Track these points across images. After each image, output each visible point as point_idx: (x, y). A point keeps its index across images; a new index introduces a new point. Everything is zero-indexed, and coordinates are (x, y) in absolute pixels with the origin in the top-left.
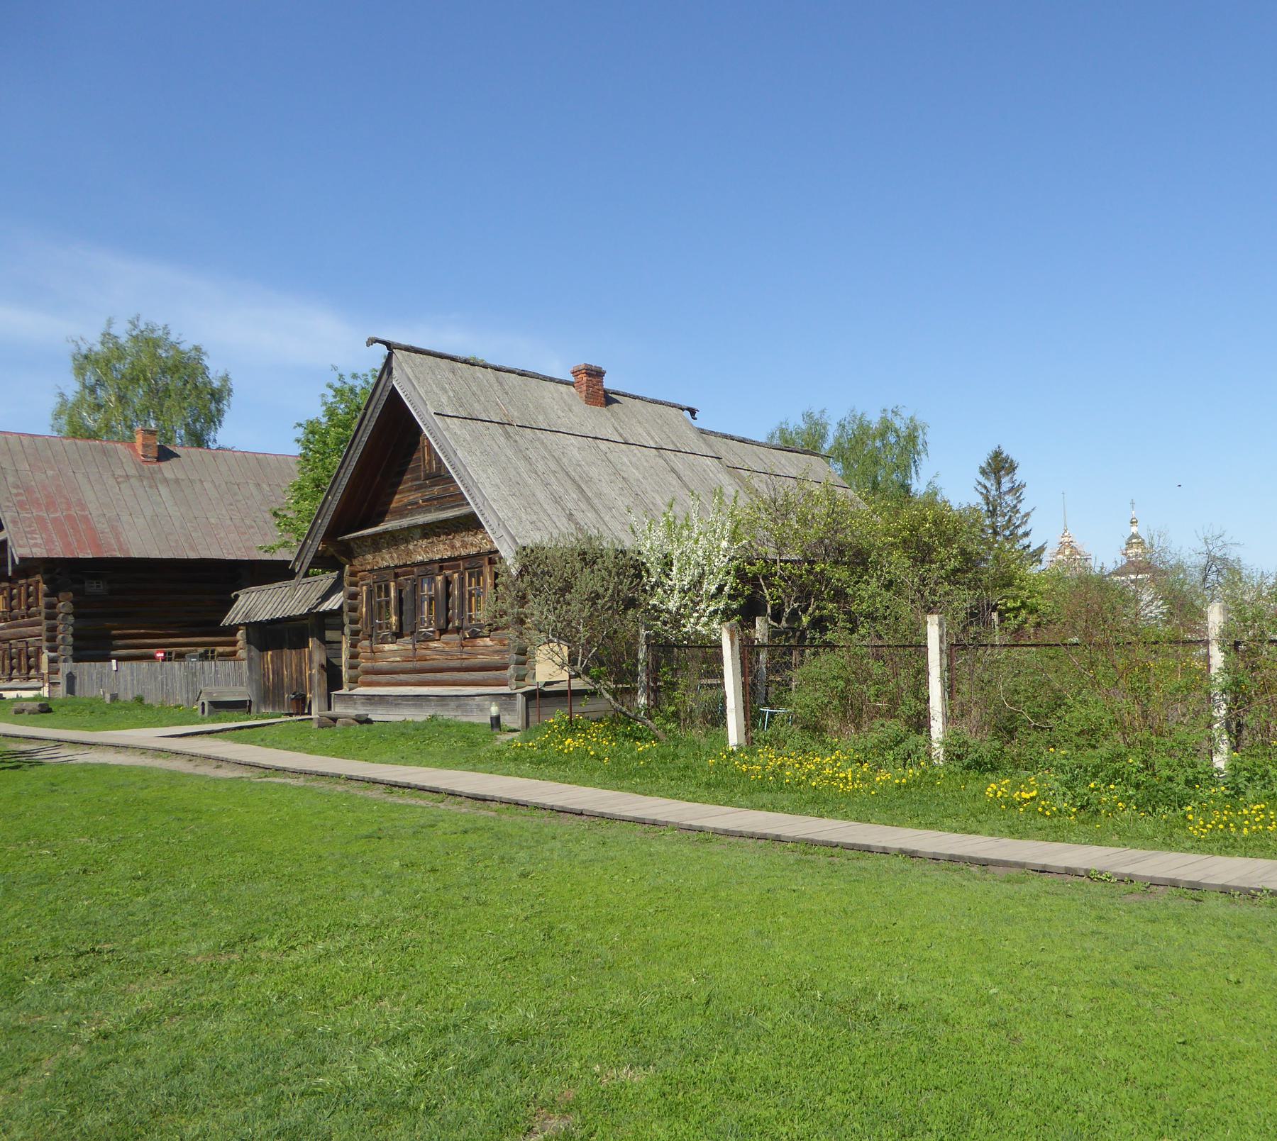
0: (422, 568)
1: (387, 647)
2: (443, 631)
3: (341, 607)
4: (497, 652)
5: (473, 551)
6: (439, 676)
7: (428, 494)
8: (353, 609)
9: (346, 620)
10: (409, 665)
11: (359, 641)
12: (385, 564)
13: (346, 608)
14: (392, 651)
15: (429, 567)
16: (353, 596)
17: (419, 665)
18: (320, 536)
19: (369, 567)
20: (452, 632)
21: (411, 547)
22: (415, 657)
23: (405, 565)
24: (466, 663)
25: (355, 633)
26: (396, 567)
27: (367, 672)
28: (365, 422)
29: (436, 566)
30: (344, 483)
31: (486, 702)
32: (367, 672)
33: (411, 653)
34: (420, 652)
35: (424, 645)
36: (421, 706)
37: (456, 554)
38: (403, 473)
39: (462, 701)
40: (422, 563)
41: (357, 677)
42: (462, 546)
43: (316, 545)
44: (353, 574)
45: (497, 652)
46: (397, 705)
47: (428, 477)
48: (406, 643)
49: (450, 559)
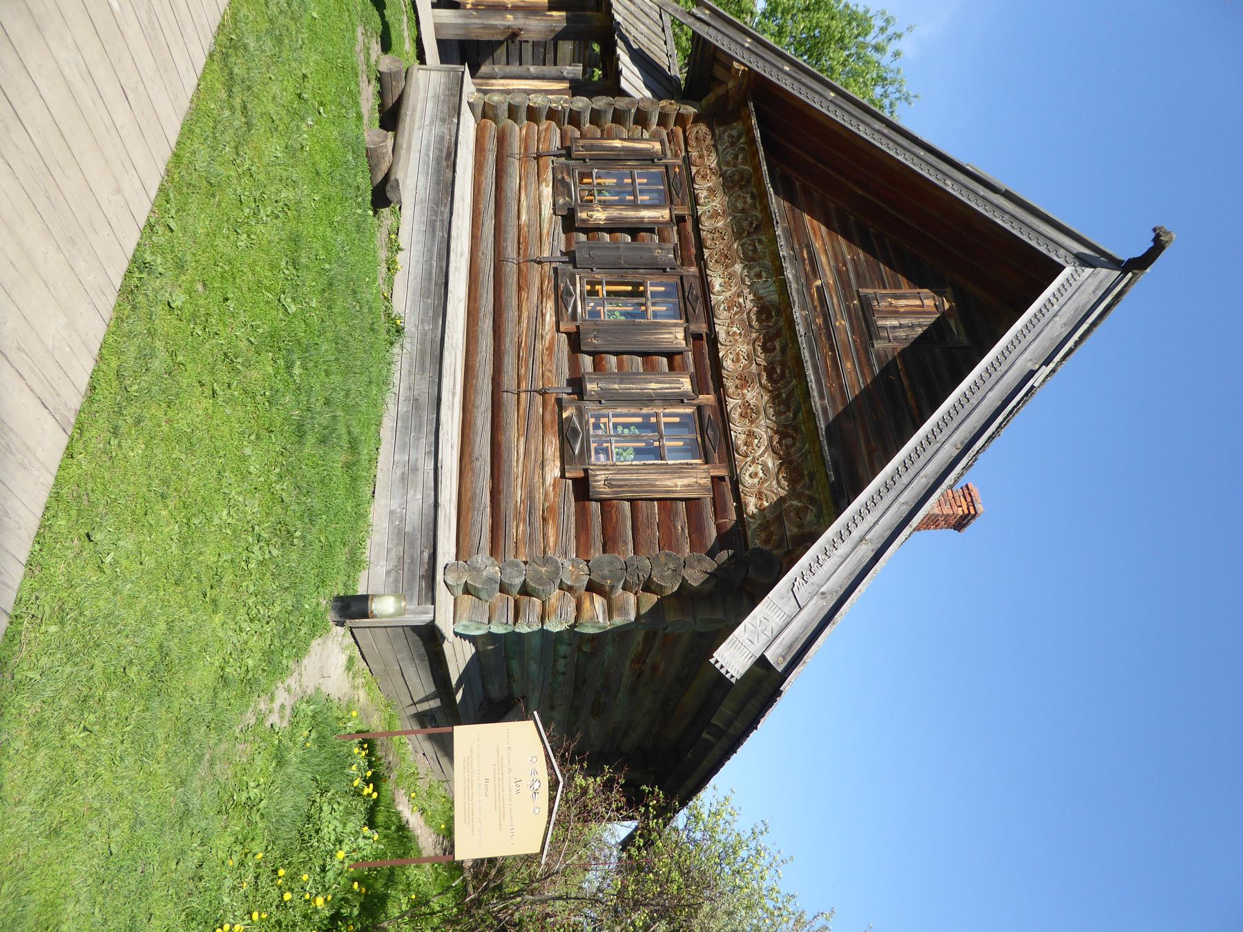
0: (697, 291)
1: (547, 191)
2: (575, 342)
3: (623, 93)
4: (530, 497)
5: (738, 431)
6: (486, 325)
7: (834, 301)
8: (619, 117)
9: (601, 102)
10: (511, 250)
11: (560, 125)
12: (702, 194)
13: (621, 103)
14: (538, 202)
15: (699, 307)
16: (642, 119)
17: (511, 270)
18: (759, 67)
19: (694, 154)
20: (574, 365)
21: (738, 267)
22: (528, 261)
23: (700, 244)
24: (509, 400)
25: (575, 118)
26: (697, 221)
27: (502, 139)
28: (982, 191)
29: (703, 328)
30: (863, 132)
31: (417, 501)
32: (502, 139)
33: (534, 253)
34: (535, 273)
35: (548, 286)
36: (425, 294)
37: (730, 384)
38: (868, 250)
39: (427, 416)
40: (706, 288)
41: (495, 119)
42: (746, 405)
43: (744, 57)
44: (681, 120)
45: (530, 497)
46: (432, 225)
47: (865, 304)
48: (553, 243)
49: (717, 364)
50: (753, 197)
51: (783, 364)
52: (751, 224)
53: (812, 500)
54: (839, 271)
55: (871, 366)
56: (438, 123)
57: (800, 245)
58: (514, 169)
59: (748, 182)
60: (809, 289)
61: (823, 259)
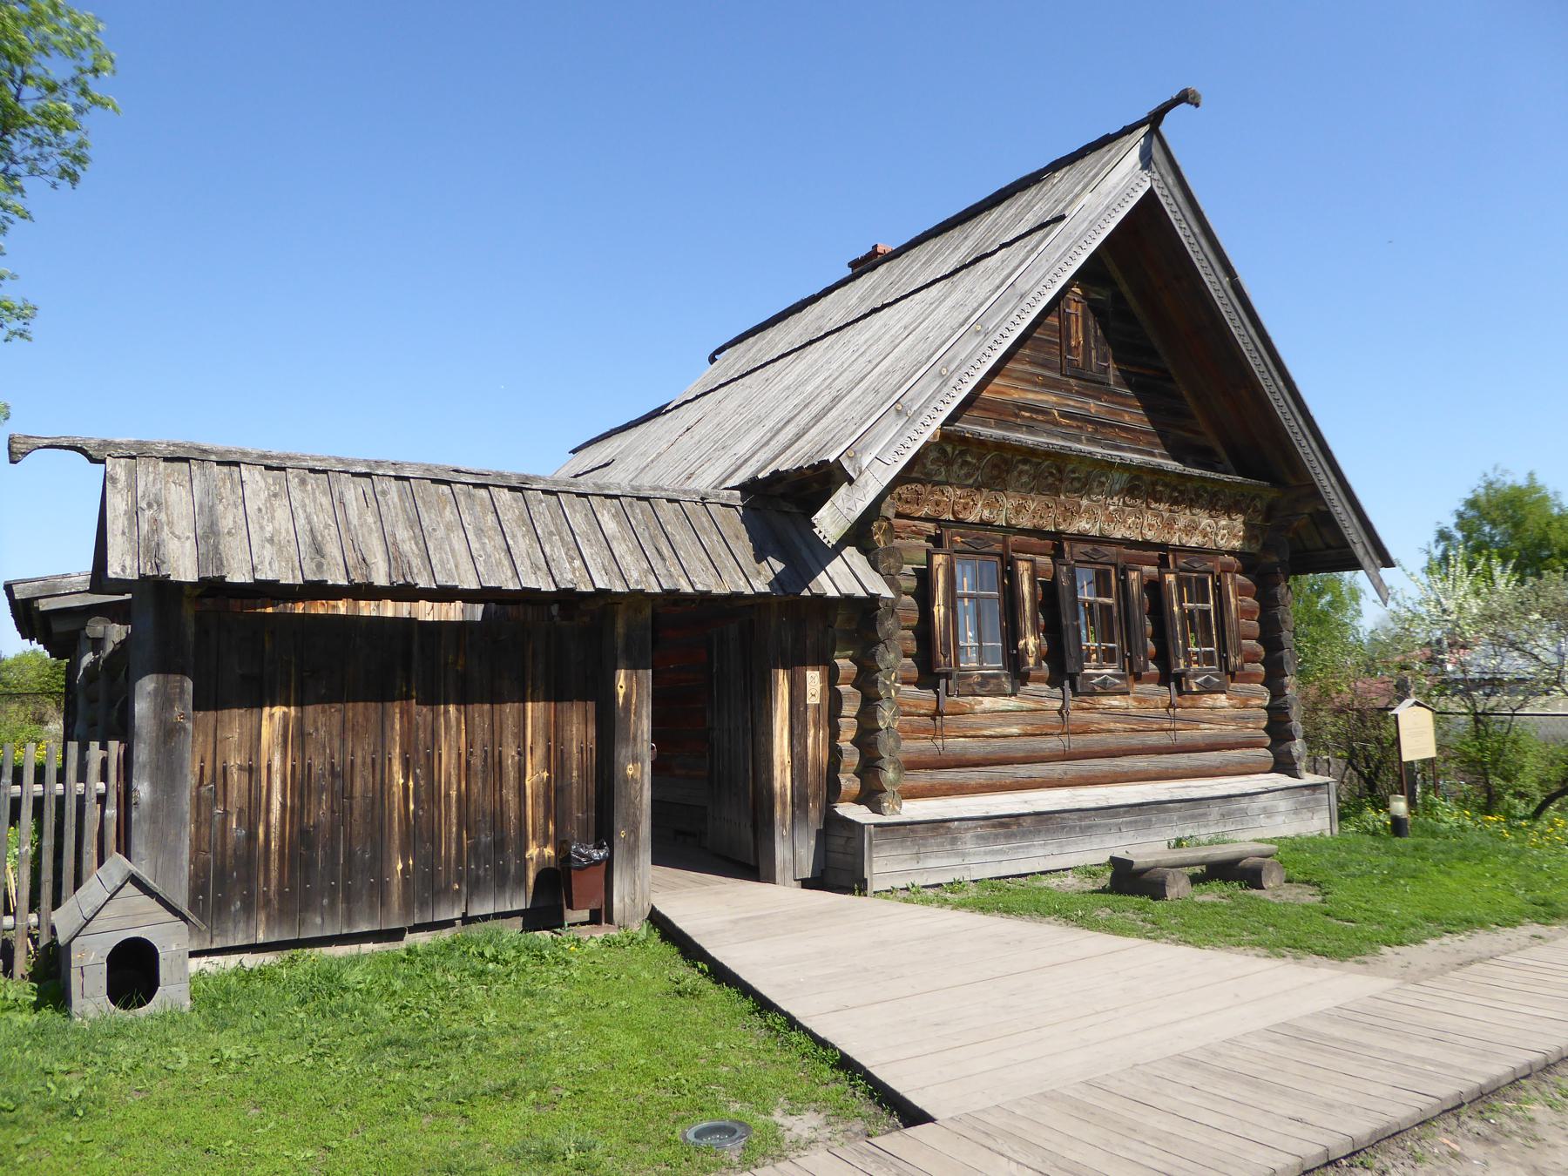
1: (988, 703)
6: (1125, 763)
10: (1053, 744)
17: (1078, 742)
21: (1085, 502)
22: (1064, 724)
27: (913, 765)
32: (913, 765)
36: (1148, 825)
46: (1085, 830)
50: (1025, 462)
51: (1175, 489)
52: (1051, 474)
53: (1253, 499)
54: (1044, 385)
55: (1126, 396)
56: (959, 846)
57: (1017, 416)
58: (1186, 735)
59: (1005, 462)
60: (1057, 424)
61: (1030, 396)
